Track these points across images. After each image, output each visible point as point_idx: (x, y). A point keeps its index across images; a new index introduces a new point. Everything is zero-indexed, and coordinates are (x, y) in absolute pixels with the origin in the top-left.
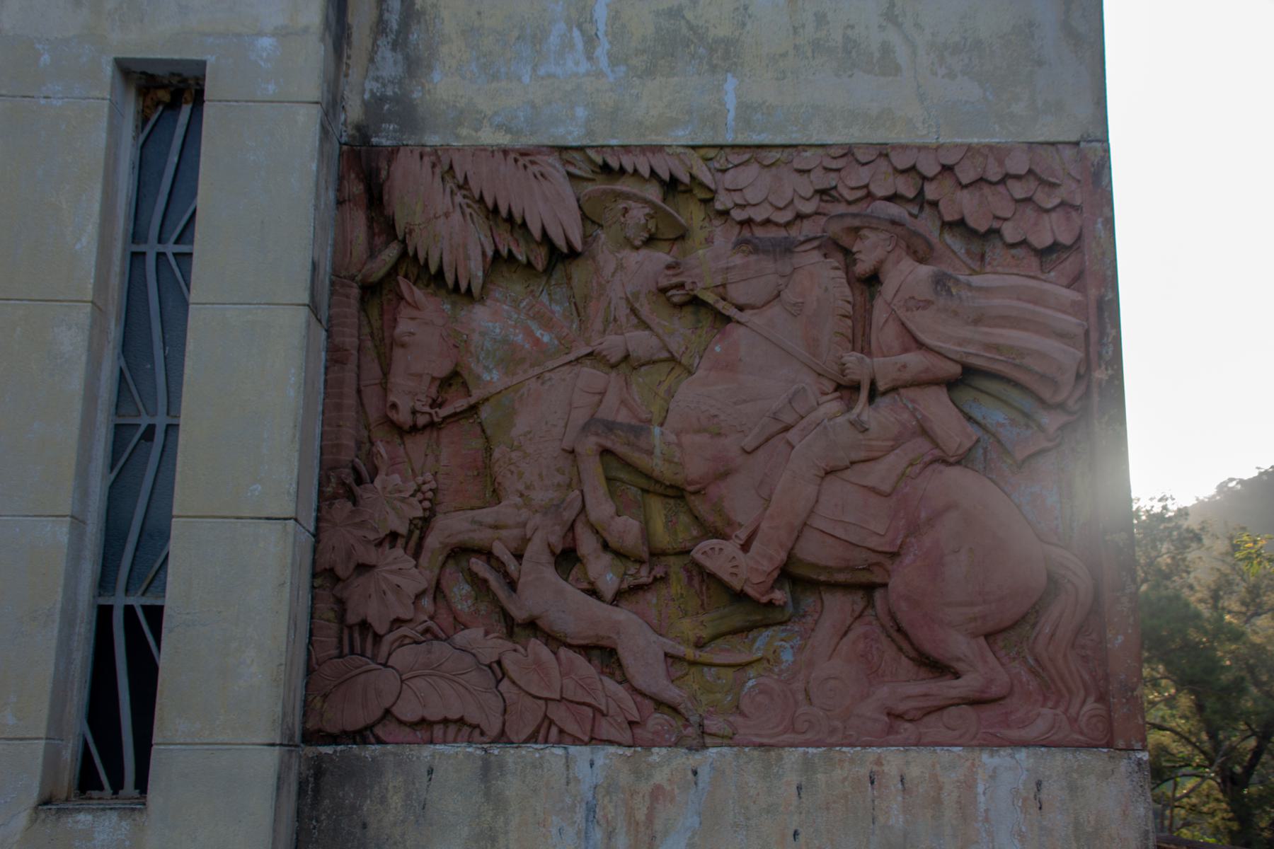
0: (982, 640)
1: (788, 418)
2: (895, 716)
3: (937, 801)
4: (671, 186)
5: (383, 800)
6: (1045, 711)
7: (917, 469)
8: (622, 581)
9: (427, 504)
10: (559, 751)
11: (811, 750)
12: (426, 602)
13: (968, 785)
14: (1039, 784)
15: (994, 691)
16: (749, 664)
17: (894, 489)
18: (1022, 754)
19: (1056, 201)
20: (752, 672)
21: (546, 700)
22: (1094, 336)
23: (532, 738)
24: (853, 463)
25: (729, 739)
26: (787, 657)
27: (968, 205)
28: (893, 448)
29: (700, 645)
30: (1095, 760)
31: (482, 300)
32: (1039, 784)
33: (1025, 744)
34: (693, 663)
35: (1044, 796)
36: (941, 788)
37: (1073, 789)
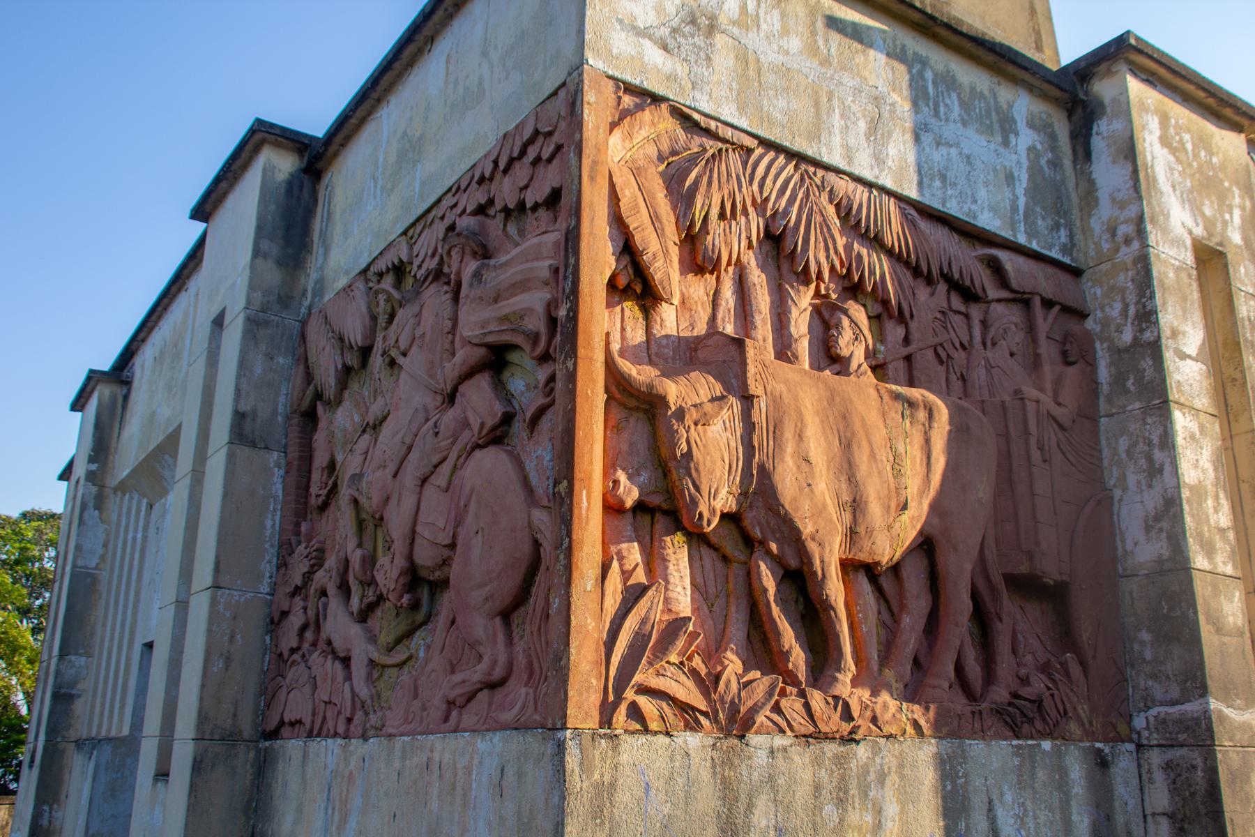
0: (498, 621)
1: (408, 441)
2: (451, 704)
3: (454, 789)
4: (399, 270)
5: (277, 782)
6: (523, 690)
7: (462, 460)
8: (361, 601)
9: (313, 561)
10: (323, 743)
11: (406, 738)
12: (309, 635)
13: (468, 770)
14: (502, 770)
15: (499, 672)
16: (404, 663)
17: (450, 483)
18: (498, 737)
19: (552, 148)
20: (406, 669)
21: (325, 702)
22: (562, 271)
23: (319, 735)
24: (436, 467)
25: (379, 730)
26: (422, 654)
27: (506, 191)
28: (453, 443)
29: (390, 650)
30: (531, 741)
31: (339, 402)
32: (502, 770)
33: (504, 727)
34: (384, 666)
35: (504, 783)
36: (456, 775)
37: (520, 774)
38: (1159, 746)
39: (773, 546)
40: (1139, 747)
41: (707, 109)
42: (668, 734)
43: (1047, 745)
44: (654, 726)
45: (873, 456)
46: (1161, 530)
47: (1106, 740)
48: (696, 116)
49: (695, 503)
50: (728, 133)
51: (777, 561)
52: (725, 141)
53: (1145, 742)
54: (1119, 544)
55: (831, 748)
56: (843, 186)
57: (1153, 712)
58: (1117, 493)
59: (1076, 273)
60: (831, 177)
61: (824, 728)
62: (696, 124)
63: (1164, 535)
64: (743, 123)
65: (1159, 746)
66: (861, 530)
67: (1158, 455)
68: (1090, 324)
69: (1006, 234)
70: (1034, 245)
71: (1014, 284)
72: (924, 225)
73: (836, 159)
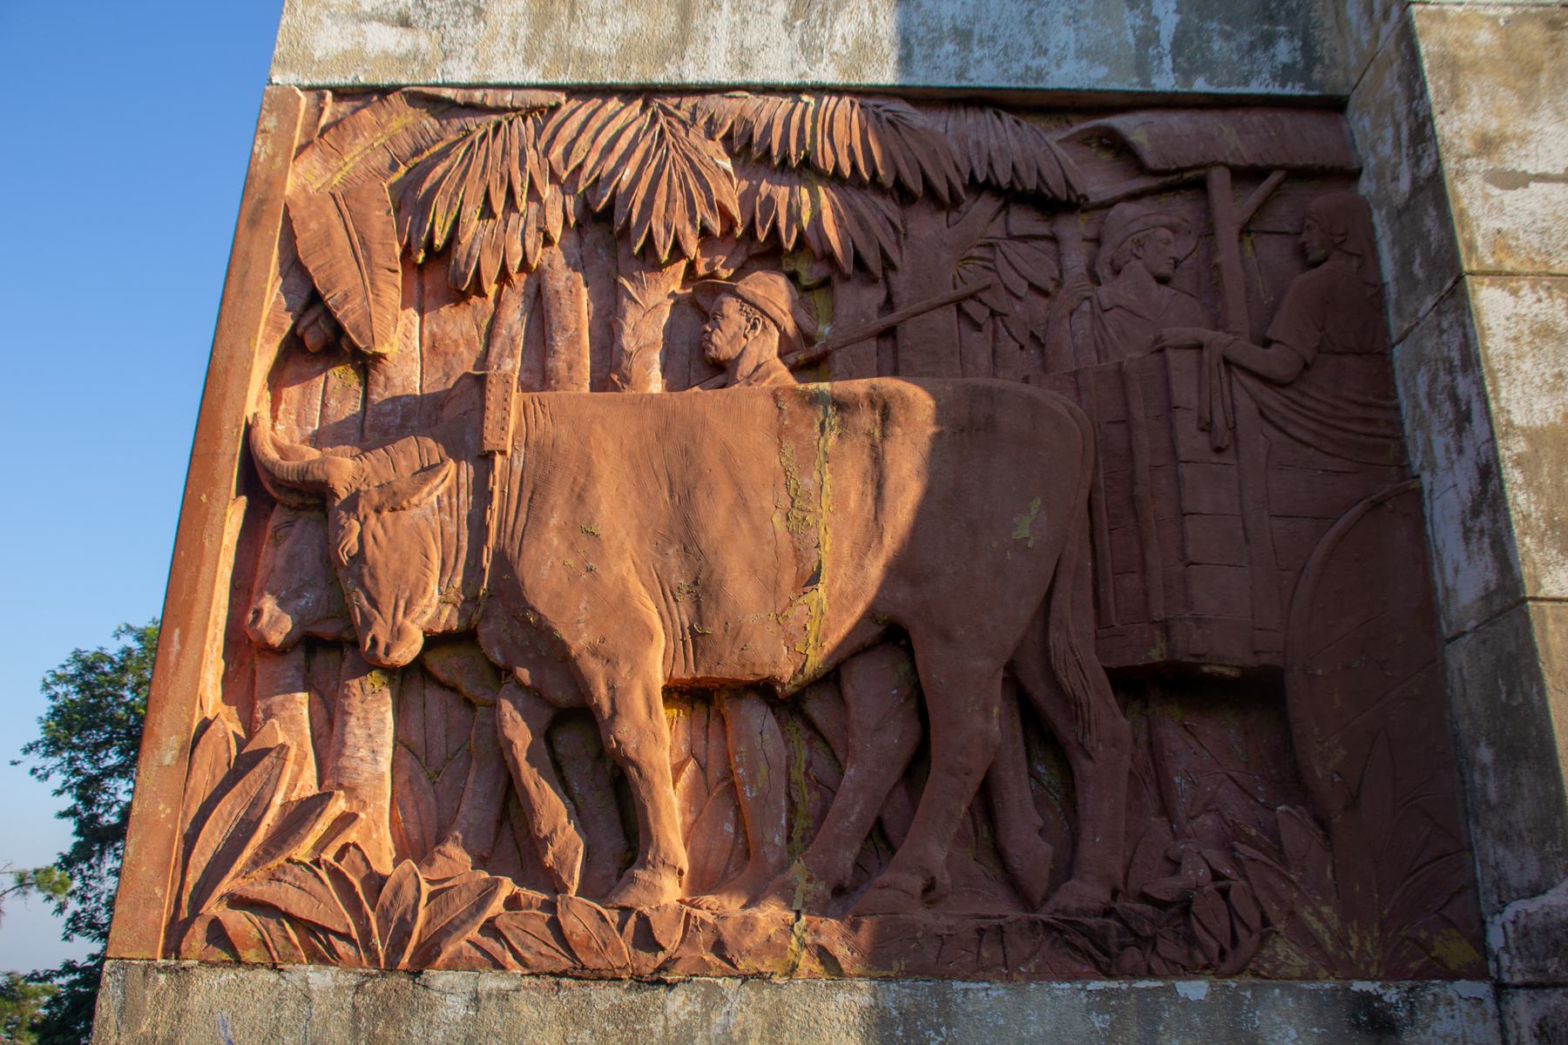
38: (1527, 986)
39: (524, 674)
40: (1501, 990)
41: (464, 77)
42: (274, 967)
43: (1195, 989)
44: (250, 955)
45: (742, 504)
46: (1482, 532)
47: (1392, 974)
48: (448, 93)
49: (368, 623)
50: (508, 98)
51: (533, 697)
52: (504, 110)
53: (1506, 978)
54: (1437, 578)
55: (604, 996)
56: (727, 109)
57: (1509, 912)
58: (1426, 478)
59: (1334, 106)
60: (713, 103)
61: (592, 962)
62: (451, 103)
63: (1486, 540)
64: (534, 76)
65: (1527, 986)
66: (714, 628)
67: (1463, 385)
68: (1366, 186)
69: (1132, 84)
70: (1200, 85)
71: (1151, 160)
72: (919, 119)
73: (719, 73)
